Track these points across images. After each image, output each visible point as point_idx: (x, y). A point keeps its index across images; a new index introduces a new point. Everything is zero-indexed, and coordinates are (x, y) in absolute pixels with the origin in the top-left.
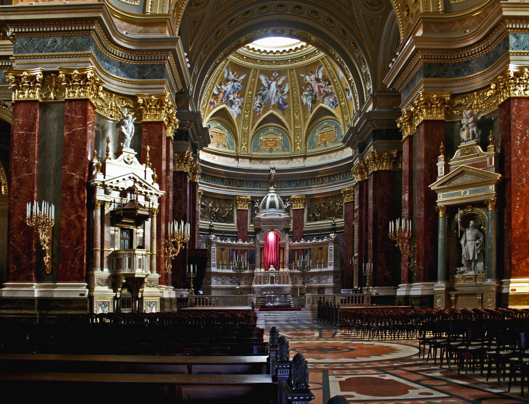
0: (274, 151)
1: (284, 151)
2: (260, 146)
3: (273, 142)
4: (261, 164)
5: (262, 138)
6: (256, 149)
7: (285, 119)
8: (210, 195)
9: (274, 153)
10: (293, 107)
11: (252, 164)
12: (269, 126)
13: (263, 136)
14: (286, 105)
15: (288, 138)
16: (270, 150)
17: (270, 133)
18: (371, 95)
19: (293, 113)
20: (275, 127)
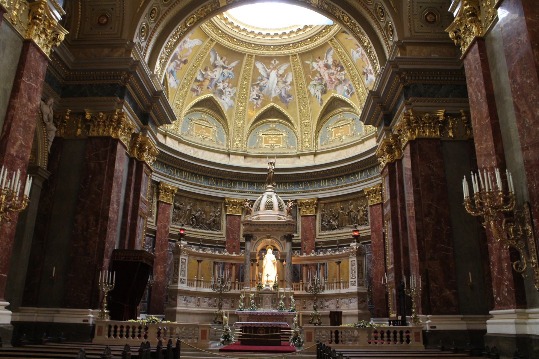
0: (276, 149)
1: (289, 148)
2: (258, 143)
3: (275, 139)
4: (260, 163)
5: (260, 135)
6: (253, 147)
7: (289, 113)
8: (188, 195)
9: (278, 151)
10: (299, 98)
11: (247, 162)
12: (270, 122)
13: (262, 132)
14: (290, 96)
15: (294, 135)
16: (271, 147)
17: (271, 130)
18: (395, 42)
19: (299, 106)
20: (277, 122)
